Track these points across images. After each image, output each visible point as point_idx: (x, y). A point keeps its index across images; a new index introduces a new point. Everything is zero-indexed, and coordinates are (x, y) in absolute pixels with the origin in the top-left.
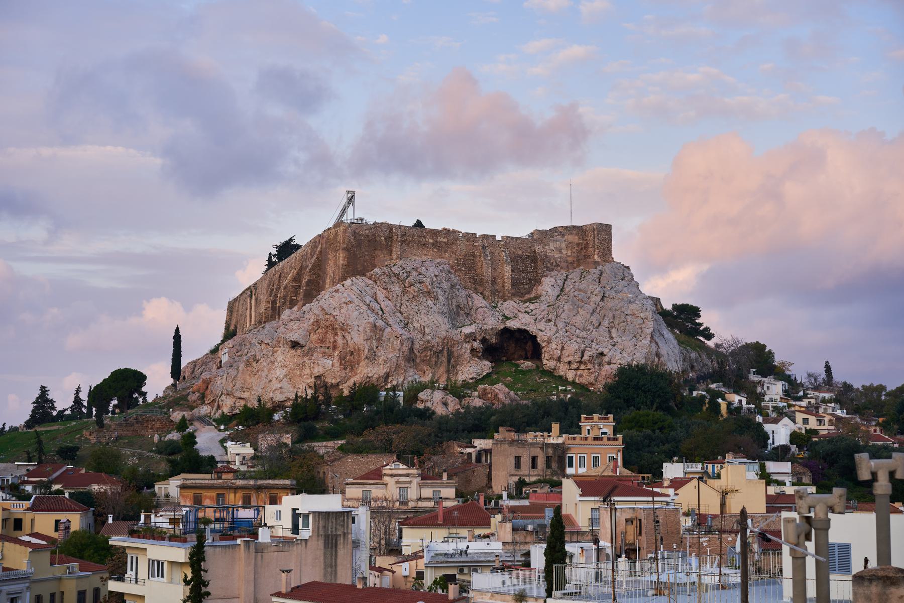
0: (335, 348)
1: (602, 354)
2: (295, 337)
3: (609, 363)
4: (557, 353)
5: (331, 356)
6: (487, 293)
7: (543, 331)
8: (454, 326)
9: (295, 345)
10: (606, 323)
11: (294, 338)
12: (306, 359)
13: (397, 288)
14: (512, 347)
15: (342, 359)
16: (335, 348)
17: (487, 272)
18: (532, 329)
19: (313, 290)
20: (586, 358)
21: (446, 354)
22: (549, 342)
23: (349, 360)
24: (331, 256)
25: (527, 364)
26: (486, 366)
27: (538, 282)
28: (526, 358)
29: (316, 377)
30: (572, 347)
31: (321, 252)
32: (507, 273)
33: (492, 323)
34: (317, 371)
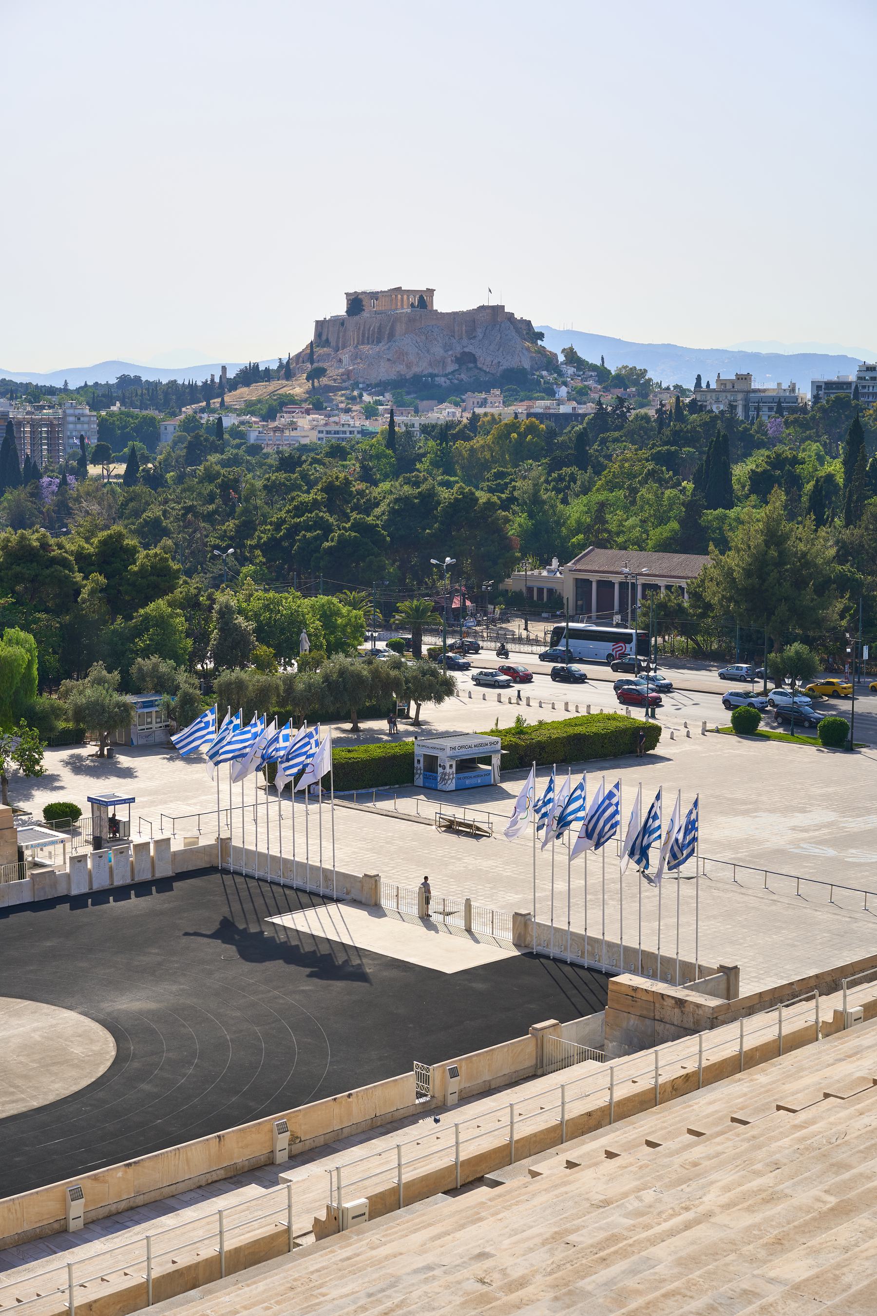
1: (499, 362)
6: (456, 337)
7: (478, 352)
8: (446, 351)
10: (501, 349)
13: (424, 337)
14: (466, 359)
15: (407, 366)
17: (456, 329)
18: (473, 352)
19: (391, 335)
21: (443, 362)
23: (409, 366)
24: (398, 324)
25: (471, 365)
26: (456, 367)
28: (471, 362)
30: (489, 359)
32: (464, 328)
33: (459, 349)
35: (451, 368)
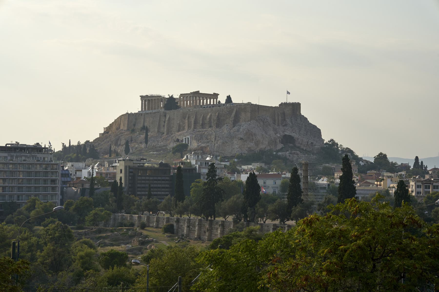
0: (253, 140)
2: (242, 136)
3: (315, 145)
4: (301, 142)
5: (253, 142)
9: (241, 139)
11: (242, 137)
12: (245, 143)
13: (262, 123)
16: (253, 140)
17: (276, 118)
18: (293, 134)
20: (309, 144)
22: (298, 139)
27: (285, 120)
29: (249, 148)
31: (236, 111)
32: (280, 118)
34: (249, 146)
35: (280, 146)
